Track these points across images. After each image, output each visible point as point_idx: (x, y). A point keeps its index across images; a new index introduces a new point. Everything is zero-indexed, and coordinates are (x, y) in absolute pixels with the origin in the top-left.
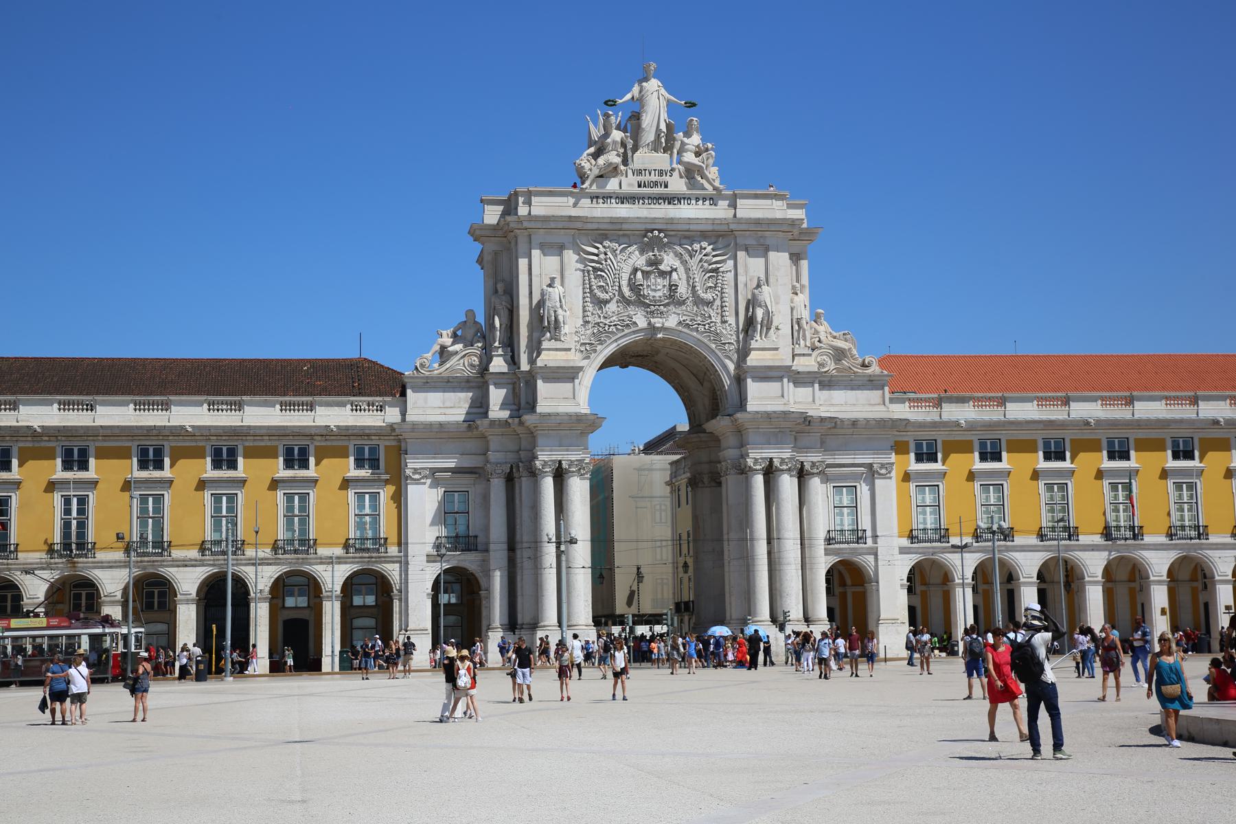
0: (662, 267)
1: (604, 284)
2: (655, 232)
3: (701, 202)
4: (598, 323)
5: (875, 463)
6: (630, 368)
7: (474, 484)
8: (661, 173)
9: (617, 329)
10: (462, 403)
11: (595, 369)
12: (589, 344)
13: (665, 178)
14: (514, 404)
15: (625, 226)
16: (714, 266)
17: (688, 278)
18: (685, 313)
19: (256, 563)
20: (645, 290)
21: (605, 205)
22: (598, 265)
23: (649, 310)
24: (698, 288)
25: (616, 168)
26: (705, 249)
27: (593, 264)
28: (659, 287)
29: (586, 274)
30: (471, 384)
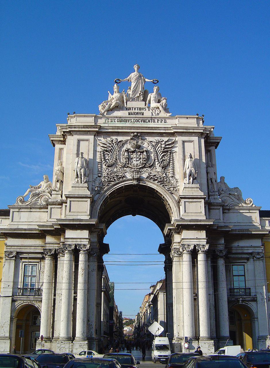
1: (109, 158)
2: (135, 133)
4: (105, 177)
5: (255, 253)
6: (138, 216)
8: (140, 109)
11: (102, 199)
12: (99, 187)
13: (142, 111)
16: (166, 150)
18: (151, 172)
21: (112, 123)
22: (106, 149)
23: (131, 170)
26: (161, 141)
29: (100, 154)
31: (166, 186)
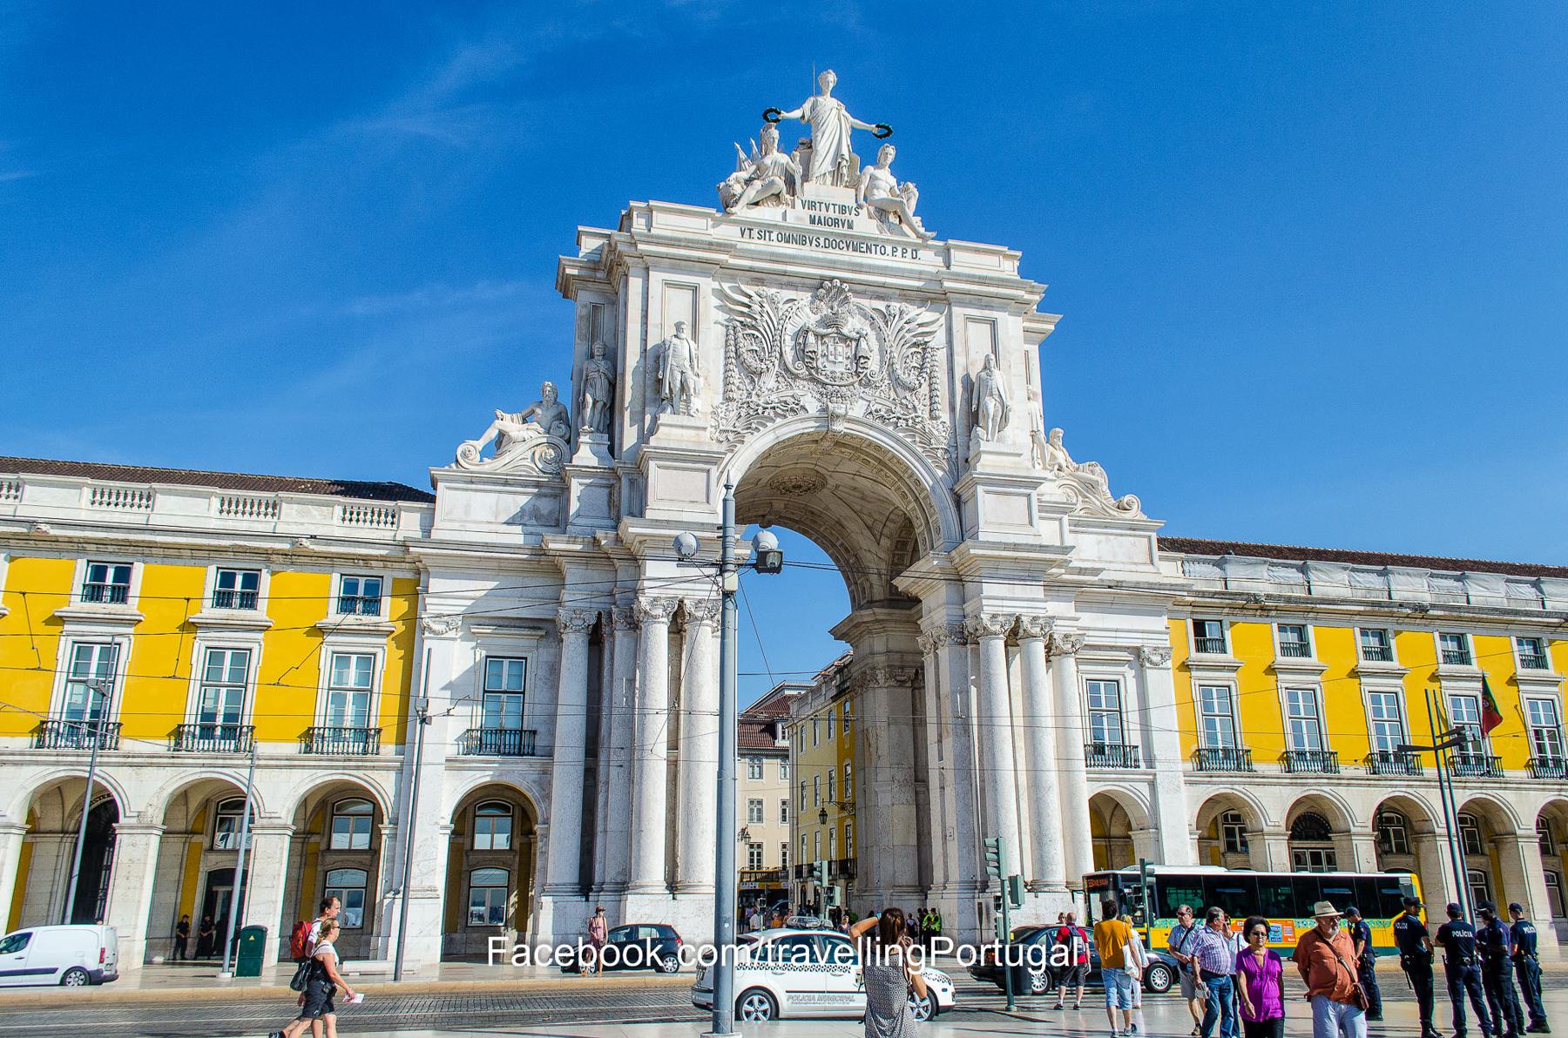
0: (845, 331)
3: (899, 253)
7: (537, 647)
8: (843, 209)
9: (776, 414)
10: (526, 518)
14: (610, 518)
15: (790, 268)
16: (921, 338)
17: (882, 352)
18: (878, 400)
19: (136, 763)
20: (821, 360)
21: (762, 241)
22: (749, 320)
24: (897, 366)
25: (777, 196)
27: (742, 319)
28: (840, 359)
30: (543, 490)
31: (920, 442)
